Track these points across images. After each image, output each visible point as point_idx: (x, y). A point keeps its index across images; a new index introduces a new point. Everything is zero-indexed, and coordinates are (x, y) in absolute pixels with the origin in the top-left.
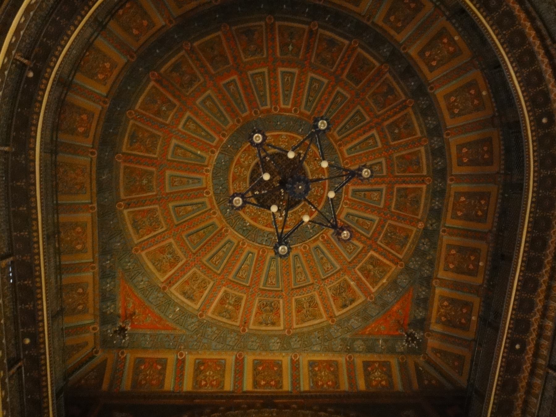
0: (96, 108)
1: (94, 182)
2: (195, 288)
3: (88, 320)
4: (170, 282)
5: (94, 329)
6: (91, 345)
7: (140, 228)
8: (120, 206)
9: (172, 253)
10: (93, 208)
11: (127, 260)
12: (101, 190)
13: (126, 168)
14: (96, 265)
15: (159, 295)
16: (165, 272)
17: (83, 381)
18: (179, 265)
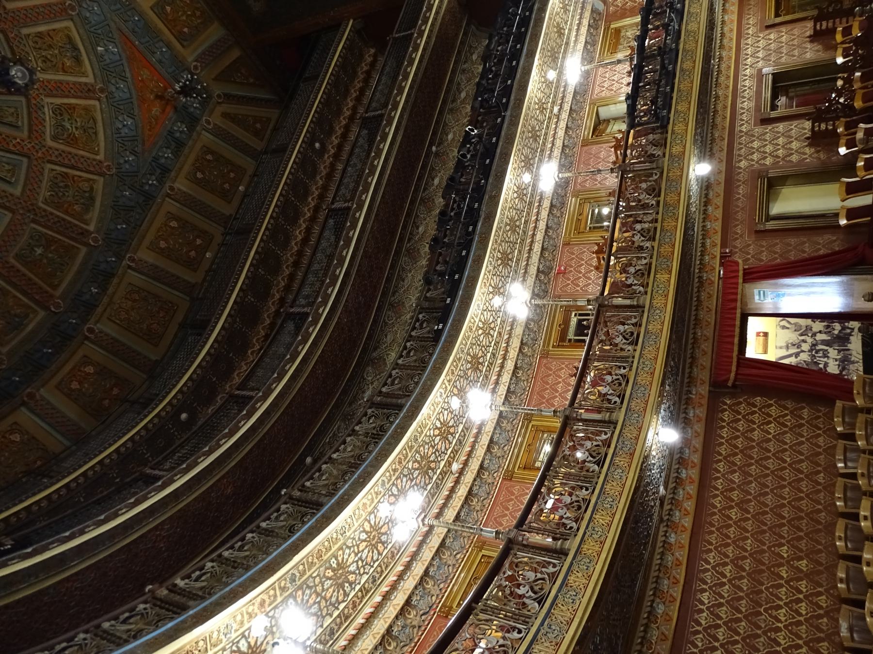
0: (48, 394)
1: (111, 290)
2: (56, 52)
3: (207, 138)
4: (87, 91)
5: (208, 122)
6: (219, 110)
7: (85, 192)
8: (95, 240)
9: (59, 126)
10: (132, 259)
11: (127, 166)
12: (109, 276)
13: (55, 287)
14: (166, 189)
15: (114, 90)
16: (86, 109)
17: (251, 80)
18: (58, 101)
